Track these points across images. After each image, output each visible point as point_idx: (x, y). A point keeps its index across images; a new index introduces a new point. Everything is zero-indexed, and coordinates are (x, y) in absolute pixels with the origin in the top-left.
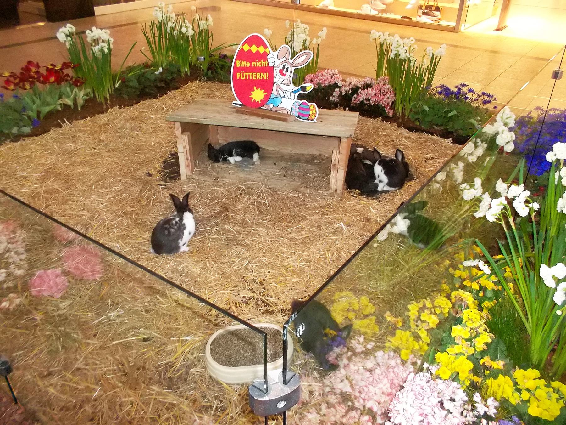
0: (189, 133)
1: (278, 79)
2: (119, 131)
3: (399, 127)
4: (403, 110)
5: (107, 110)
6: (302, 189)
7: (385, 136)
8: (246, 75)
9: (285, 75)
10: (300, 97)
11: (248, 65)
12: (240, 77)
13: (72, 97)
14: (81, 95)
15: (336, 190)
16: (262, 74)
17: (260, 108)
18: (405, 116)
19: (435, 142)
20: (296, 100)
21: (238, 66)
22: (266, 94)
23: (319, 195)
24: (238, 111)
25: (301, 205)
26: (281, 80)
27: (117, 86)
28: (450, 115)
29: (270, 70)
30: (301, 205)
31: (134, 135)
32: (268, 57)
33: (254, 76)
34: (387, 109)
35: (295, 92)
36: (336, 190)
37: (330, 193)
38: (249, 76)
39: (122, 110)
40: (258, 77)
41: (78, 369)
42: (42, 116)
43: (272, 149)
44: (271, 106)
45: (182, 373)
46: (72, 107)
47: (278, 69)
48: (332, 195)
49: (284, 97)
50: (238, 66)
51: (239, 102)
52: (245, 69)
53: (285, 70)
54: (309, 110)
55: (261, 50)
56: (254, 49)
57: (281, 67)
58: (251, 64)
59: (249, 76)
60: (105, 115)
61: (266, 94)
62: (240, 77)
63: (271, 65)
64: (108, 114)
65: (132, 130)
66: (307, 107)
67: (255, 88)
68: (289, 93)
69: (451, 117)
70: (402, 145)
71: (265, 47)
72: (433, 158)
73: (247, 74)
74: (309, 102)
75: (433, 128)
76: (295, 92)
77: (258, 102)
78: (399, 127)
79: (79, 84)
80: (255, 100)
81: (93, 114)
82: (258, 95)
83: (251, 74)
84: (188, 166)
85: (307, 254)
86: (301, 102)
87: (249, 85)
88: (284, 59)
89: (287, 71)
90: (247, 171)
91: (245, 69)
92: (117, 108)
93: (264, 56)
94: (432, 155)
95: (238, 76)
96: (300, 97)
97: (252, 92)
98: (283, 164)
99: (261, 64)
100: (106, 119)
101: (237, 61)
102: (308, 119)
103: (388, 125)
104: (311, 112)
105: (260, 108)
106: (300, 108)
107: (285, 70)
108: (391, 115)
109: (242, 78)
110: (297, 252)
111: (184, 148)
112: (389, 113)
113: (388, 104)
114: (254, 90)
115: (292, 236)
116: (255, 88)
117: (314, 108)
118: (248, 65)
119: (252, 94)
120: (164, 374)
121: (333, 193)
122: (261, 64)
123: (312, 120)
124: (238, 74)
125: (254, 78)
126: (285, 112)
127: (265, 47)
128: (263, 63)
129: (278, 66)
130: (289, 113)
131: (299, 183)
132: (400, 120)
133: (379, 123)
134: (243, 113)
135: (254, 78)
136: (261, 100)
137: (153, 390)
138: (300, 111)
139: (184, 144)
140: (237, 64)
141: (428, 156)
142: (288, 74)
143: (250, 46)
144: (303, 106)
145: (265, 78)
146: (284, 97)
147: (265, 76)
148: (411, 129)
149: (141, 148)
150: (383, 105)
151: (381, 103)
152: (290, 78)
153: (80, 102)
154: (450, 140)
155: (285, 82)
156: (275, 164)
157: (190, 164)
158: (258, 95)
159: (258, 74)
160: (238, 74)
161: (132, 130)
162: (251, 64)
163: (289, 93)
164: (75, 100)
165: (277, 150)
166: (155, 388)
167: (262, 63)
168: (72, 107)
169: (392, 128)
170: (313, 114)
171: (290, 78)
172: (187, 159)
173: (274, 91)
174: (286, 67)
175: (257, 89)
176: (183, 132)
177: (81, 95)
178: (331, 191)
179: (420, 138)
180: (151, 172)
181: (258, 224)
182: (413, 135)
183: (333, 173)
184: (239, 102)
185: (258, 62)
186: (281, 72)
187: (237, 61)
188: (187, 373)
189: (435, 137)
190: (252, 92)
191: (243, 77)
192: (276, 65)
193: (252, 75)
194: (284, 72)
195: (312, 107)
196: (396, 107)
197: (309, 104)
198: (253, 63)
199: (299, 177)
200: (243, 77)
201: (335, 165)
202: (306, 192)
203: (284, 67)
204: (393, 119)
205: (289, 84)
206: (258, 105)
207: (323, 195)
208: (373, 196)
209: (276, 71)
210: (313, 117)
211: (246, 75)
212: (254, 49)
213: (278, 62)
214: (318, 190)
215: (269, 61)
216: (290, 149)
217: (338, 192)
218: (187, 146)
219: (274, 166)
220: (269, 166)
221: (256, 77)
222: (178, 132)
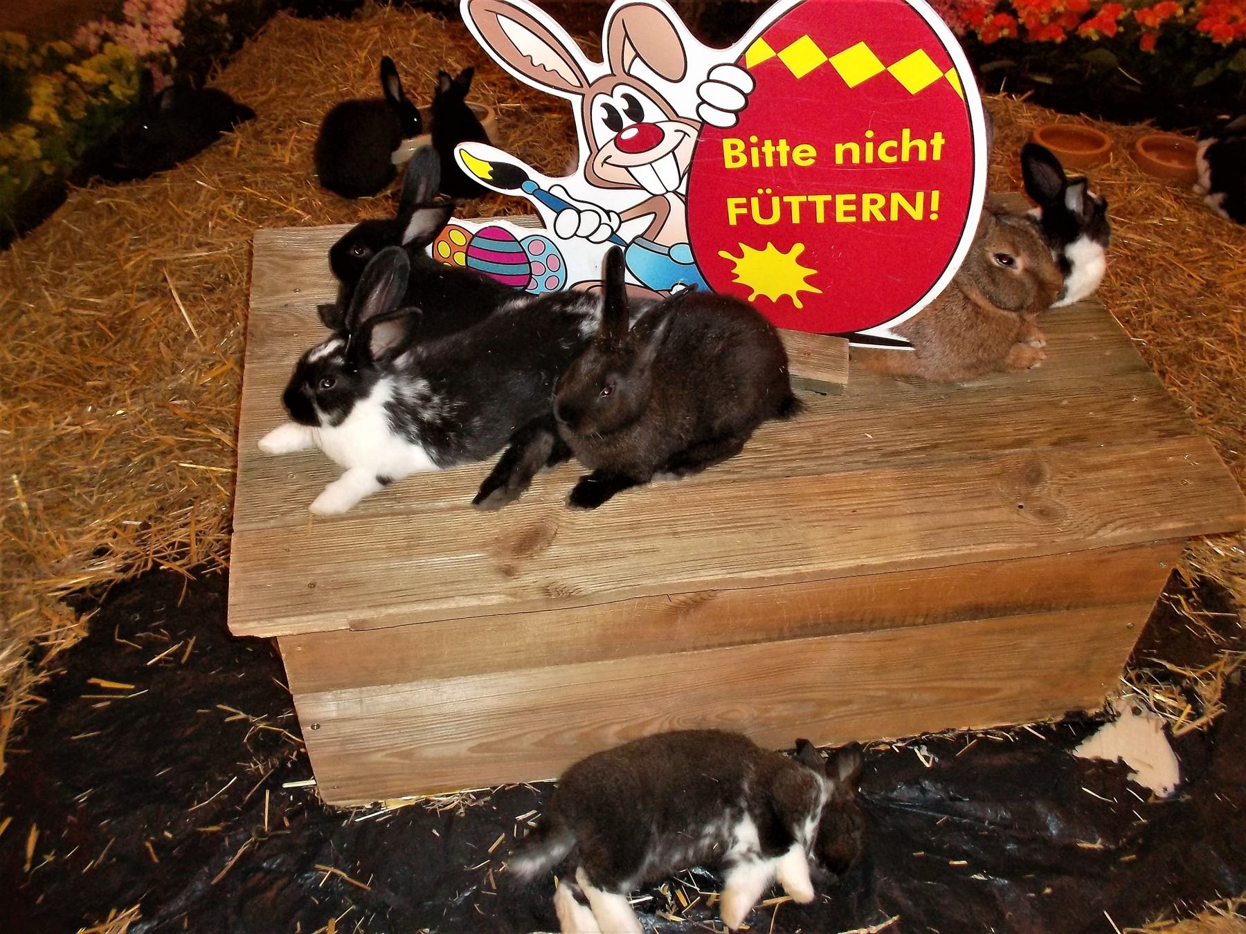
8: (786, 209)
11: (805, 155)
12: (745, 220)
16: (897, 198)
21: (729, 164)
33: (840, 208)
38: (808, 209)
50: (729, 164)
58: (826, 154)
59: (808, 209)
62: (745, 220)
73: (795, 201)
83: (820, 200)
109: (757, 217)
118: (805, 155)
124: (731, 202)
125: (840, 218)
135: (840, 218)
140: (728, 154)
145: (917, 214)
159: (866, 198)
160: (731, 202)
162: (826, 154)
167: (907, 145)
191: (766, 212)
193: (830, 208)
198: (840, 149)
200: (766, 212)
211: (786, 209)
221: (858, 213)
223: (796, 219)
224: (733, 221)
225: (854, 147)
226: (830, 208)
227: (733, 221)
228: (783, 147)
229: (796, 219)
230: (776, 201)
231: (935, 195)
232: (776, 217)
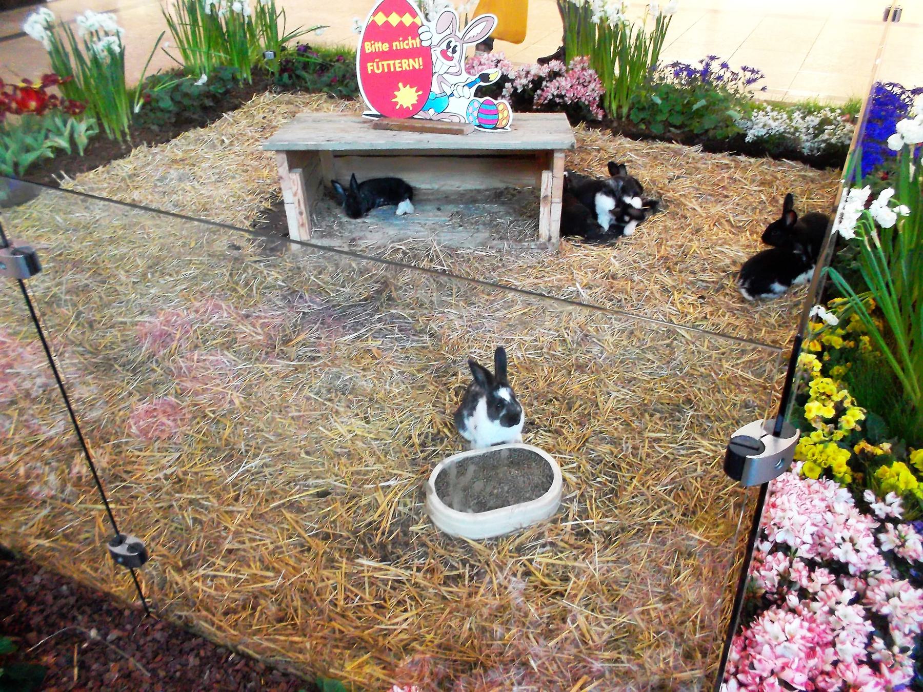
0: (300, 170)
1: (440, 65)
2: (159, 184)
3: (615, 134)
4: (620, 107)
5: (128, 151)
6: (495, 242)
7: (598, 151)
9: (451, 59)
10: (480, 92)
12: (373, 70)
13: (67, 133)
14: (83, 129)
15: (550, 239)
17: (412, 118)
18: (622, 118)
19: (677, 153)
20: (472, 97)
21: (367, 51)
22: (420, 93)
23: (522, 250)
24: (377, 127)
25: (498, 267)
26: (445, 69)
27: (137, 110)
28: (695, 107)
29: (424, 53)
30: (498, 267)
31: (188, 188)
32: (420, 31)
33: (397, 65)
34: (593, 109)
35: (470, 85)
36: (550, 239)
37: (541, 244)
38: (389, 65)
39: (154, 150)
40: (405, 67)
41: (230, 551)
42: (21, 170)
43: (428, 186)
44: (431, 112)
45: (398, 534)
46: (69, 151)
47: (439, 50)
48: (543, 247)
49: (452, 95)
50: (367, 51)
51: (374, 112)
52: (383, 56)
53: (451, 50)
54: (496, 112)
55: (407, 20)
56: (394, 19)
57: (444, 46)
58: (391, 47)
59: (389, 65)
60: (127, 160)
61: (420, 93)
62: (373, 70)
63: (425, 44)
64: (131, 158)
65: (180, 179)
66: (493, 108)
67: (400, 85)
68: (460, 88)
69: (698, 110)
70: (628, 161)
71: (414, 14)
72: (678, 177)
73: (385, 63)
74: (496, 99)
75: (669, 131)
76: (470, 85)
77: (408, 108)
78: (615, 134)
79: (77, 110)
80: (401, 106)
81: (107, 161)
82: (406, 96)
83: (391, 62)
84: (303, 225)
85: (532, 338)
86: (482, 100)
87: (392, 80)
88: (448, 32)
89: (454, 51)
90: (397, 225)
91: (383, 56)
92: (144, 148)
93: (413, 31)
94: (677, 173)
95: (370, 69)
96: (480, 92)
97: (396, 93)
98: (452, 208)
99: (408, 44)
100: (131, 166)
101: (366, 43)
102: (495, 128)
103: (597, 133)
104: (500, 116)
105: (412, 118)
106: (481, 111)
107: (451, 50)
108: (600, 117)
109: (376, 71)
110: (517, 338)
111: (295, 194)
112: (597, 113)
113: (594, 99)
114: (398, 90)
115: (499, 314)
116: (400, 85)
117: (505, 108)
118: (385, 48)
119: (395, 97)
120: (370, 540)
121: (544, 244)
122: (408, 44)
123: (503, 128)
124: (369, 64)
125: (398, 69)
126: (456, 120)
127: (414, 14)
128: (411, 43)
129: (438, 45)
130: (463, 121)
131: (487, 234)
132: (615, 124)
133: (583, 132)
134: (386, 128)
136: (413, 105)
137: (362, 565)
138: (483, 116)
139: (295, 189)
140: (367, 47)
141: (671, 175)
142: (456, 56)
143: (387, 15)
144: (484, 107)
145: (417, 67)
146: (452, 95)
147: (416, 64)
148: (634, 137)
149: (208, 206)
150: (587, 103)
151: (583, 100)
152: (460, 61)
153: (82, 140)
154: (699, 147)
155: (451, 70)
156: (439, 209)
157: (305, 221)
158: (406, 96)
159: (404, 61)
160: (369, 64)
161: (180, 179)
162: (391, 47)
163: (460, 88)
164: (72, 140)
165: (436, 186)
166: (364, 561)
168: (69, 151)
169: (606, 137)
170: (503, 119)
171: (460, 61)
172: (301, 213)
173: (435, 88)
174: (452, 45)
175: (405, 86)
176: (291, 167)
177: (83, 129)
178: (542, 240)
179: (651, 148)
180: (237, 243)
181: (443, 303)
182: (639, 144)
183: (544, 210)
184: (374, 112)
185: (403, 41)
186: (444, 53)
187: (366, 43)
188: (405, 533)
189: (675, 146)
190: (396, 93)
191: (378, 68)
192: (435, 43)
193: (394, 64)
194: (449, 54)
195: (500, 108)
196: (606, 104)
197: (495, 102)
198: (394, 44)
199: (484, 224)
200: (378, 68)
201: (546, 197)
202: (501, 247)
203: (448, 46)
204: (603, 125)
205: (459, 74)
206: (408, 114)
207: (529, 248)
208: (606, 242)
209: (436, 54)
210: (504, 122)
212: (394, 19)
213: (436, 39)
214: (520, 241)
215: (422, 37)
216: (457, 184)
217: (554, 240)
218: (300, 193)
219: (439, 213)
220: (431, 214)
221: (401, 67)
222: (283, 169)
223: (386, 70)
224: (370, 72)
225: (397, 43)
226: (394, 64)
227: (370, 72)
228: (380, 44)
229: (386, 70)
230: (380, 64)
231: (421, 59)
232: (380, 71)
